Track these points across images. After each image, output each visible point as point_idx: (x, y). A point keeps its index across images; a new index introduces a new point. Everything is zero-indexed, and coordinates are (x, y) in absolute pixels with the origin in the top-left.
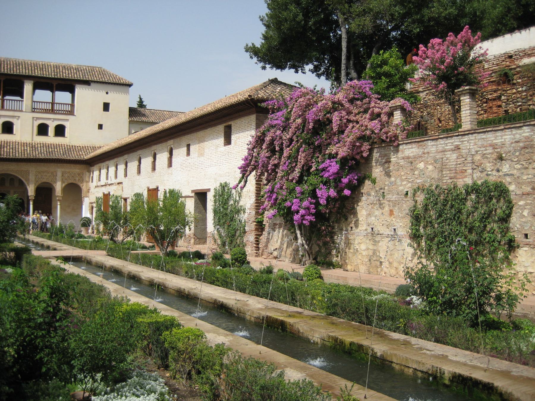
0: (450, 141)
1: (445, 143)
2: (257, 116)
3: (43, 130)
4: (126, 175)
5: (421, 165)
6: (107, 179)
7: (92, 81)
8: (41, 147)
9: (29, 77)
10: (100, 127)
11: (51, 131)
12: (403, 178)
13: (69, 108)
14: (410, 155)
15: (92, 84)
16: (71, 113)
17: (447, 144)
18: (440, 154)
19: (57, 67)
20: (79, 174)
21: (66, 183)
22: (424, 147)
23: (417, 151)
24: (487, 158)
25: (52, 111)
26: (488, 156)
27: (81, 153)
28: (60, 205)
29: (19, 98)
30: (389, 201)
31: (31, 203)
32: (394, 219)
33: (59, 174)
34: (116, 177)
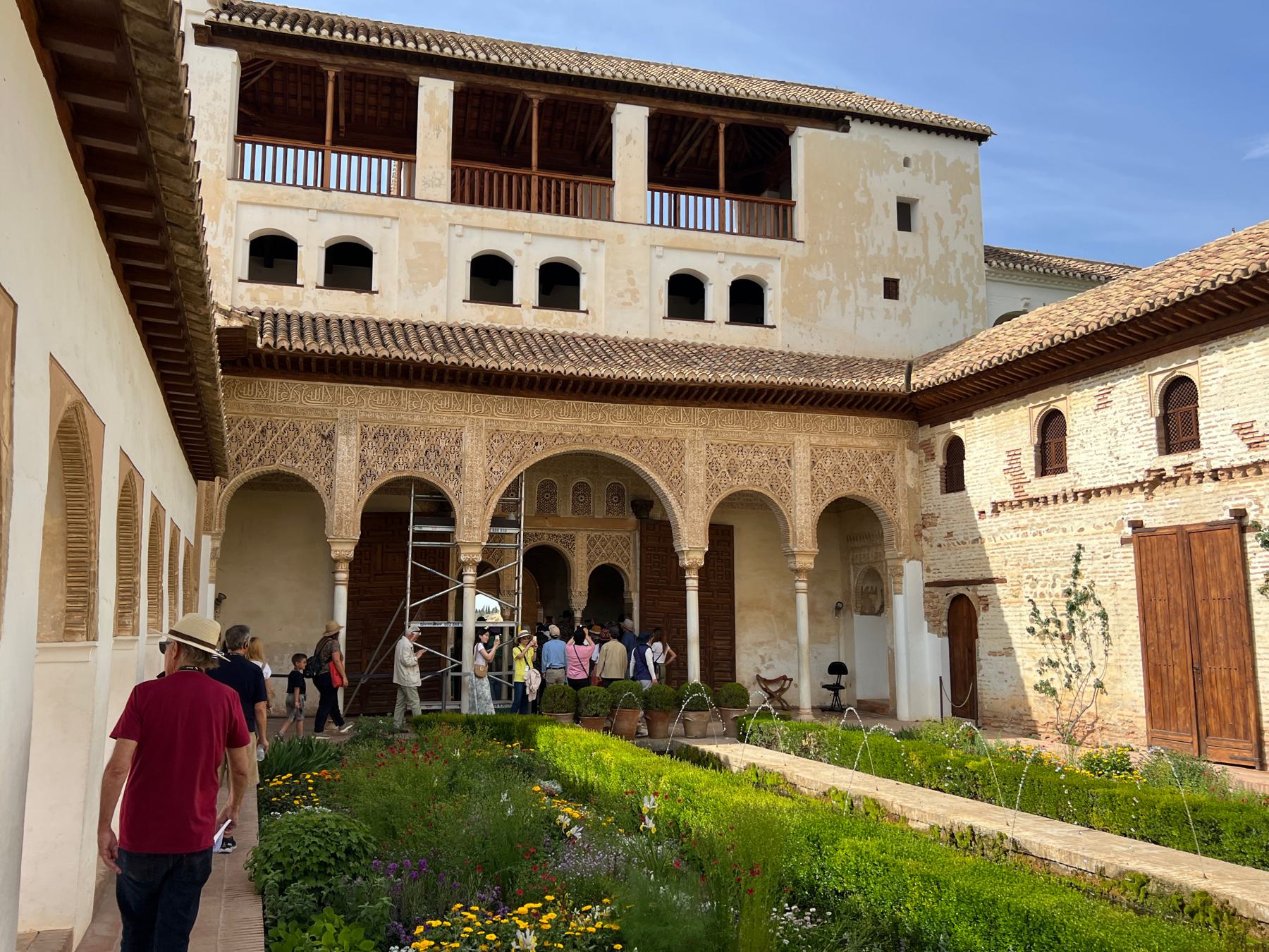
21: (828, 501)
28: (809, 591)
31: (692, 583)
33: (802, 457)
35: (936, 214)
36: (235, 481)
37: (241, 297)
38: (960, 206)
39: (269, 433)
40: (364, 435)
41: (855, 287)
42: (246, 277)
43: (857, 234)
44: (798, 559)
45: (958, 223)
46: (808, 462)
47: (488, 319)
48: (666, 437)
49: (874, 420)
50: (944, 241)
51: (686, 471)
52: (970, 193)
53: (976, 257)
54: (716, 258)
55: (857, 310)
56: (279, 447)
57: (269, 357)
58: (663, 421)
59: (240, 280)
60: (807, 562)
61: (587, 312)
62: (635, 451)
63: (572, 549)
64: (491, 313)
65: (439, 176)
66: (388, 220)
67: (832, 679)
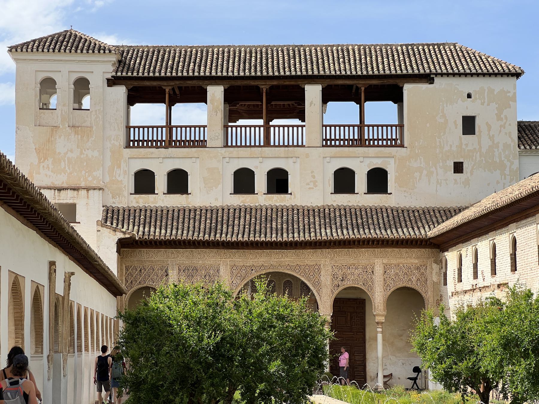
3: (344, 181)
4: (514, 268)
6: (476, 276)
7: (436, 74)
8: (340, 216)
9: (313, 79)
10: (458, 168)
11: (361, 182)
13: (394, 134)
15: (437, 80)
19: (366, 51)
20: (418, 268)
21: (392, 290)
25: (361, 142)
28: (382, 333)
29: (297, 122)
33: (379, 270)
34: (494, 272)
35: (487, 123)
36: (129, 293)
37: (132, 202)
38: (502, 116)
39: (143, 271)
40: (179, 270)
41: (436, 169)
42: (133, 192)
43: (438, 140)
44: (377, 318)
45: (501, 126)
46: (382, 272)
47: (242, 202)
48: (312, 264)
49: (416, 250)
50: (491, 138)
51: (322, 279)
52: (510, 107)
53: (512, 144)
54: (359, 160)
55: (438, 182)
56: (147, 277)
57: (141, 242)
58: (310, 256)
59: (131, 194)
60: (382, 319)
61: (291, 194)
62: (297, 271)
64: (243, 199)
65: (217, 134)
66: (194, 159)
67: (414, 375)
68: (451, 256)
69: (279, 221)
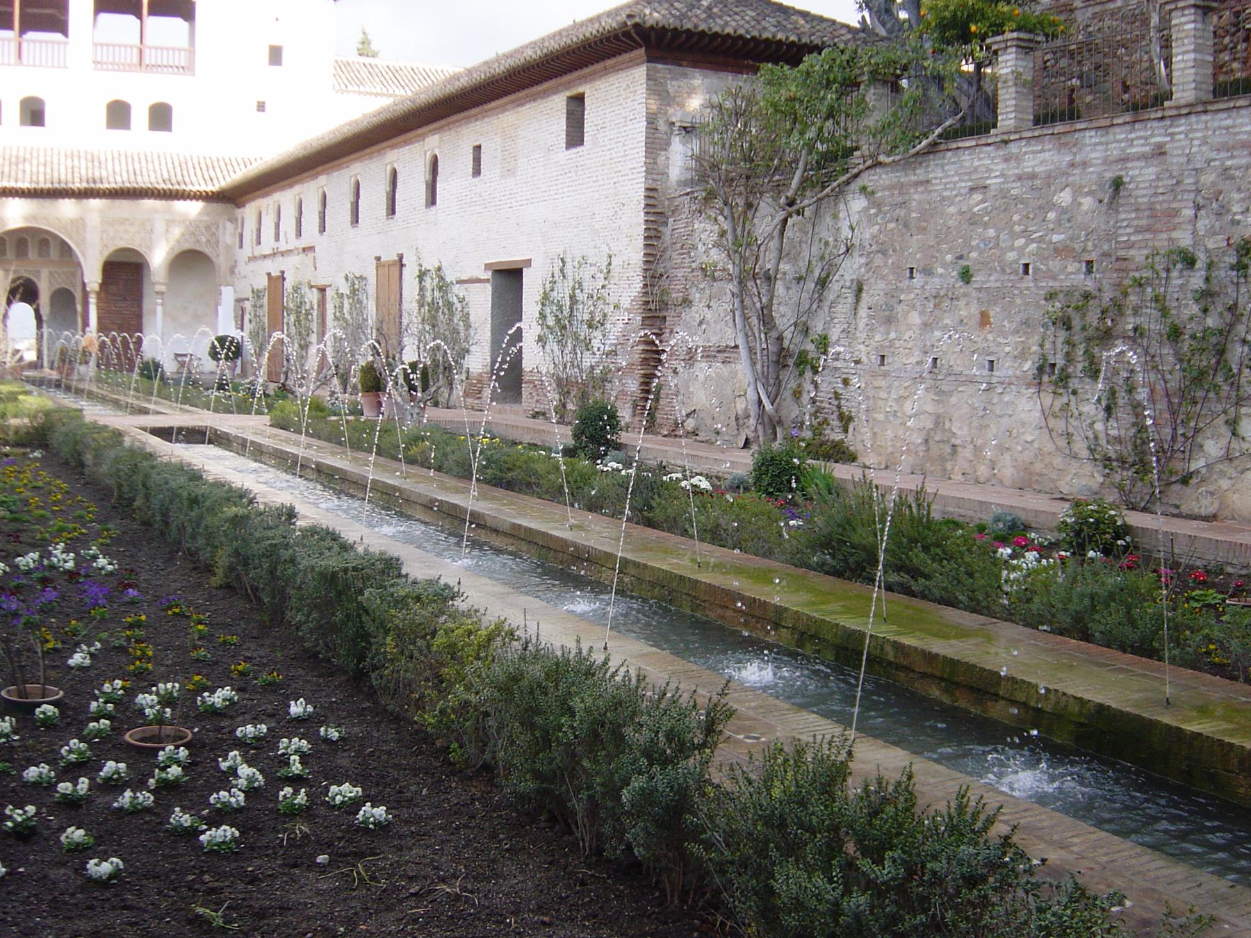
0: (1140, 132)
1: (1127, 139)
2: (648, 70)
3: (118, 114)
4: (323, 229)
5: (1065, 198)
11: (140, 117)
12: (1017, 228)
14: (1037, 170)
16: (188, 69)
17: (1132, 140)
18: (1114, 167)
20: (208, 228)
22: (1074, 150)
23: (1055, 159)
24: (1233, 178)
26: (1237, 173)
27: (213, 175)
29: (58, 36)
30: (979, 290)
31: (93, 300)
32: (990, 337)
63: (39, 279)
68: (249, 212)
69: (35, 162)
